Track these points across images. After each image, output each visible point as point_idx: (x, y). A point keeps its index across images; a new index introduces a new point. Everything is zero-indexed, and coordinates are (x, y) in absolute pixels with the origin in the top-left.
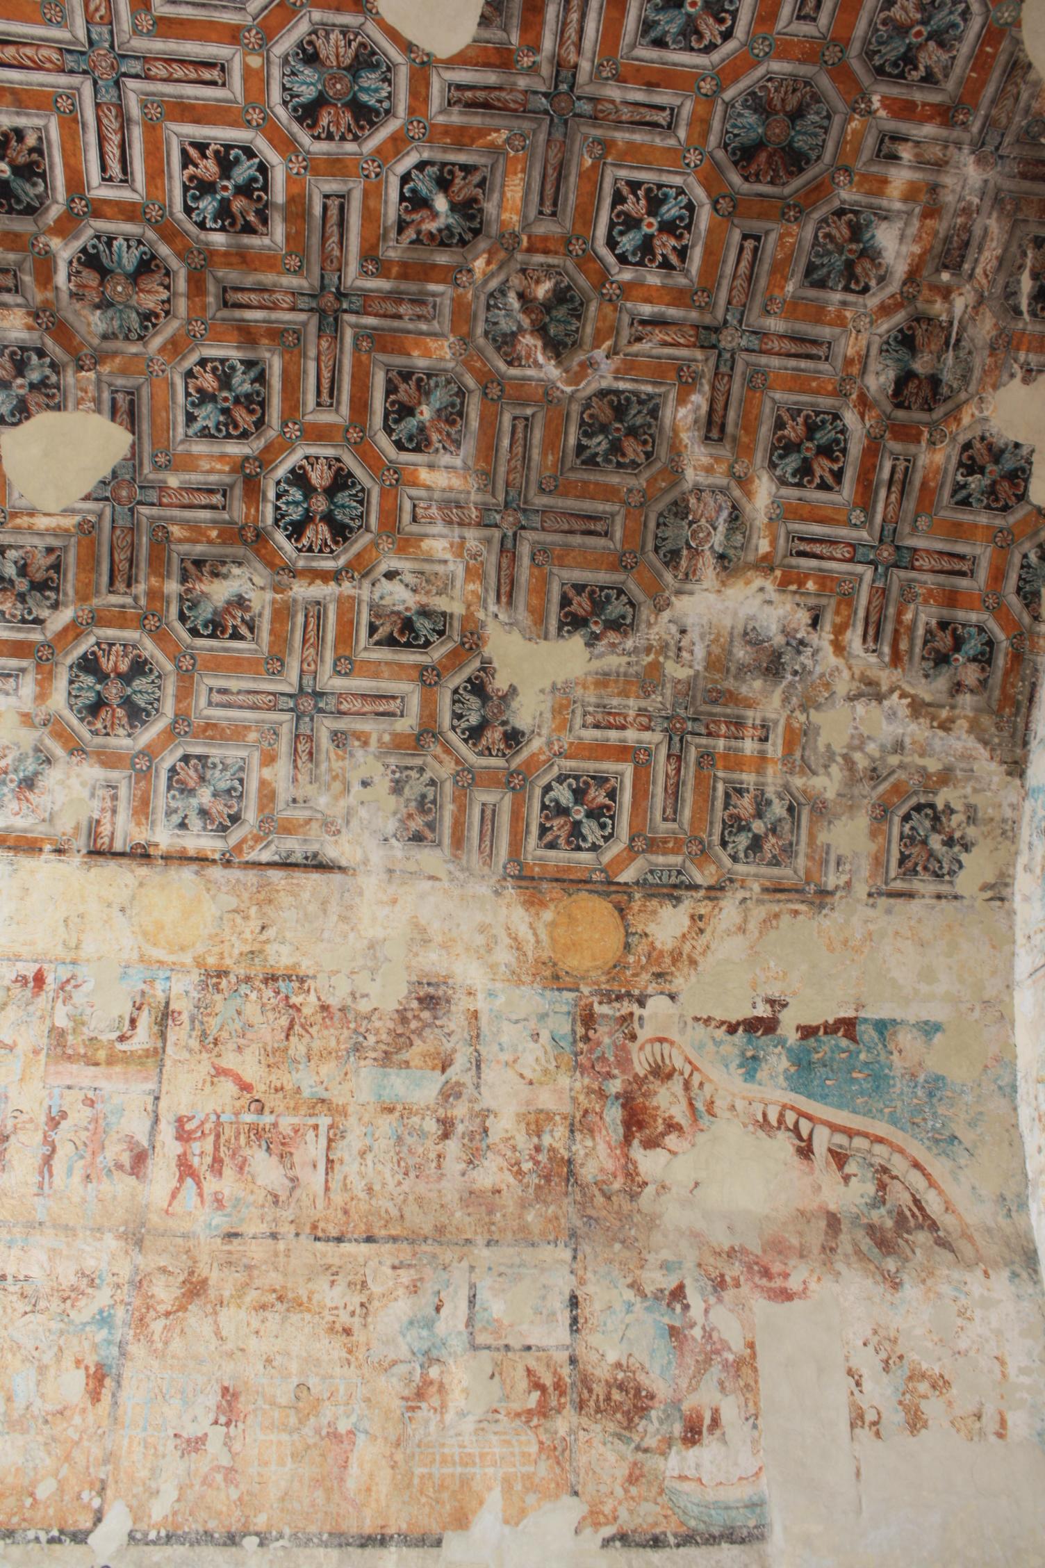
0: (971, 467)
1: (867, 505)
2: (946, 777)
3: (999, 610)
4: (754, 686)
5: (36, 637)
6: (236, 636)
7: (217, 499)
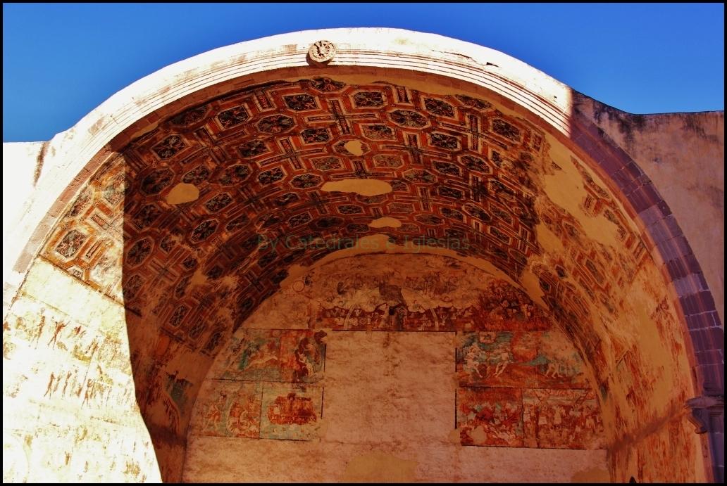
0: (279, 273)
1: (262, 273)
2: (225, 329)
3: (257, 299)
4: (218, 298)
5: (138, 232)
6: (167, 250)
7: (193, 219)
